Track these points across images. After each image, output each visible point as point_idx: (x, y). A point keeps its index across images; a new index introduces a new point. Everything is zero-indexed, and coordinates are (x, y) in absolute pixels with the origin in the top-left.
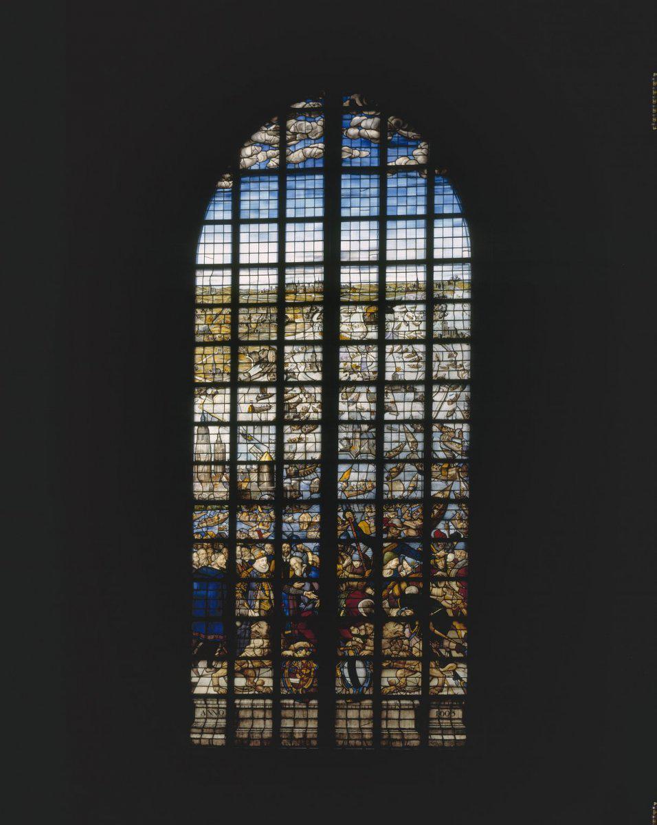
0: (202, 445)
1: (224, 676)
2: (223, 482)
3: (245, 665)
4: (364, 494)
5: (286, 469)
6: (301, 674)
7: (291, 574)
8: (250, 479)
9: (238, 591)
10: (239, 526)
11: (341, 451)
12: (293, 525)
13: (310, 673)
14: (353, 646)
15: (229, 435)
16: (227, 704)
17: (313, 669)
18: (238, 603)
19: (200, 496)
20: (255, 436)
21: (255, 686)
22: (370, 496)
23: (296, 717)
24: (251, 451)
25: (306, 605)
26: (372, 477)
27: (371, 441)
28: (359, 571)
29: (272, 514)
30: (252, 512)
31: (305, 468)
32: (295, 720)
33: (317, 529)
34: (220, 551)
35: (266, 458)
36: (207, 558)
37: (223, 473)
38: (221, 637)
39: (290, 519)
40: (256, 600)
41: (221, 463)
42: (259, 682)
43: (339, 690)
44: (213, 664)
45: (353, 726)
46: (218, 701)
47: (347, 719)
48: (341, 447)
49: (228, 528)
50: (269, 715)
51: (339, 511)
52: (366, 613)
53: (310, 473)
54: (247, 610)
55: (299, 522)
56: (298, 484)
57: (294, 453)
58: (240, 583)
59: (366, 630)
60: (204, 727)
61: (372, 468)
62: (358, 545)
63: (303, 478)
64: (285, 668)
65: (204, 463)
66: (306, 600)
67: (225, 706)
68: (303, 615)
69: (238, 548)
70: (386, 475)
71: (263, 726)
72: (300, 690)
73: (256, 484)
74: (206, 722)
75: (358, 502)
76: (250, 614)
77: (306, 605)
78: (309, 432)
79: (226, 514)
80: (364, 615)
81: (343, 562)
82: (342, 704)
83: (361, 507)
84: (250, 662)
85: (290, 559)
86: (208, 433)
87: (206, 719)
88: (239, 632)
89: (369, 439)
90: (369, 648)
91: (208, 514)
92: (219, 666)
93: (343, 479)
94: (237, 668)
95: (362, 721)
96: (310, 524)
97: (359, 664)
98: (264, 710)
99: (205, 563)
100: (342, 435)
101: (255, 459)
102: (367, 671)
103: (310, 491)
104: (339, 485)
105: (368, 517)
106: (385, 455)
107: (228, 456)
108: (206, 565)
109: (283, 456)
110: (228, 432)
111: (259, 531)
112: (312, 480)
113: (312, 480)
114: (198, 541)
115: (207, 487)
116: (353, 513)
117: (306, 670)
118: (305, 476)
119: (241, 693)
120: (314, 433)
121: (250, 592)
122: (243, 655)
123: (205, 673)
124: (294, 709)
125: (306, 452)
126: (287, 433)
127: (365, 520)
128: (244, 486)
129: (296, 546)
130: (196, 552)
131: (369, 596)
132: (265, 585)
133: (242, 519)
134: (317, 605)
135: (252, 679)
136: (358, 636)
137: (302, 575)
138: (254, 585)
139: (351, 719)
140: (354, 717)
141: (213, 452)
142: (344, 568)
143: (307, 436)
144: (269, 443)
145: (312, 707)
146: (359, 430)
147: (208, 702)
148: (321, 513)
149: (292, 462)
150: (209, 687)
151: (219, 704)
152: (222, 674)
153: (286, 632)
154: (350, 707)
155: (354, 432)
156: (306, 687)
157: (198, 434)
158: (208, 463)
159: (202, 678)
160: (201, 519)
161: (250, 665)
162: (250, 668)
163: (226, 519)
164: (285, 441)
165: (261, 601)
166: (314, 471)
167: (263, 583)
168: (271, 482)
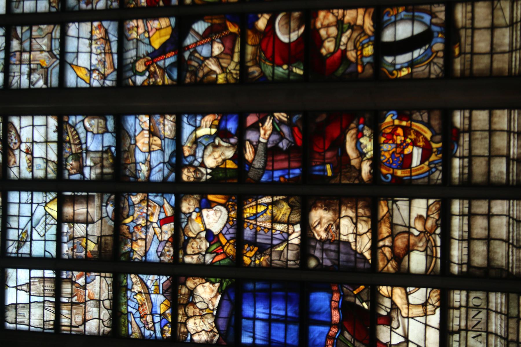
0: (32, 317)
1: (407, 294)
2: (86, 283)
3: (387, 251)
4: (110, 42)
5: (70, 174)
6: (403, 145)
7: (230, 165)
8: (82, 237)
9: (257, 262)
10: (153, 257)
11: (46, 83)
12: (154, 163)
13: (402, 127)
14: (355, 48)
15: (19, 270)
16: (461, 289)
17: (397, 122)
18: (277, 262)
19: (105, 323)
20: (22, 227)
21: (426, 233)
22: (111, 27)
23: (487, 153)
24: (42, 234)
25: (282, 137)
26: (86, 27)
27: (34, 34)
28: (228, 44)
29: (136, 199)
30: (131, 233)
31: (69, 142)
32: (491, 156)
33: (161, 120)
34: (192, 293)
35: (53, 210)
36: (202, 316)
37: (73, 283)
38: (336, 296)
39: (144, 168)
40: (272, 228)
41: (58, 282)
42: (419, 226)
43: (436, 70)
44: (384, 313)
45: (507, 41)
46: (454, 308)
47: (492, 52)
48: (40, 84)
49: (156, 277)
50: (481, 207)
51: (134, 82)
52: (299, 28)
53: (77, 134)
54: (289, 248)
55: (150, 152)
56: (92, 155)
57: (47, 161)
58: (245, 258)
59: (328, 26)
60: (506, 339)
61: (73, 29)
62: (188, 48)
63: (84, 146)
64: (393, 175)
65: (58, 314)
66: (275, 137)
67: (464, 293)
68: (299, 142)
69: (188, 259)
70: (83, 6)
71: (504, 220)
72: (434, 145)
73: (90, 226)
74: (496, 335)
75: (121, 51)
76: (296, 241)
77: (282, 137)
78: (19, 136)
79: (134, 280)
80: (302, 30)
81: (214, 72)
82: (463, 64)
83: (131, 45)
84: (381, 244)
85: (206, 168)
86: (16, 306)
87: (488, 333)
88: (327, 263)
89: (31, 38)
90: (360, 17)
91: (134, 311)
92: (387, 303)
93: (87, 78)
94: (391, 267)
95: (496, 22)
96: (152, 133)
97: (388, 36)
98: (471, 215)
99: (210, 320)
100: (25, 83)
101: (54, 227)
102: (402, 20)
103: (103, 134)
104: (95, 84)
105: (144, 32)
106: (53, 10)
107: (49, 274)
108: (213, 319)
109: (52, 181)
110: (15, 270)
111: (163, 222)
112: (87, 130)
113: (87, 130)
114: (174, 332)
115: (93, 311)
116: (138, 58)
117: (398, 135)
118: (80, 143)
119: (439, 261)
120: (21, 128)
121: (258, 240)
122: (367, 255)
123: (400, 331)
124: (471, 157)
125: (47, 142)
126: (20, 173)
127: (149, 38)
128: (92, 246)
129: (186, 158)
130: (192, 335)
131: (271, 24)
132: (249, 212)
133: (142, 253)
134: (282, 116)
135: (412, 240)
136: (338, 39)
137: (233, 145)
138: (248, 233)
139: (492, 44)
140: (489, 37)
141: (41, 299)
142: (224, 70)
143: (24, 139)
144: (32, 203)
145: (467, 122)
146: (18, 54)
147: (456, 328)
148: (136, 113)
149: (60, 165)
150: (426, 325)
151: (461, 306)
152: (404, 296)
153: (329, 173)
154: (468, 49)
155: (21, 63)
156: (428, 135)
157: (16, 323)
158: (58, 306)
159: (410, 338)
160: (141, 325)
161: (387, 242)
162: (393, 242)
163: (141, 280)
164: (28, 175)
165: (274, 220)
166: (74, 127)
167: (245, 216)
168: (88, 200)
